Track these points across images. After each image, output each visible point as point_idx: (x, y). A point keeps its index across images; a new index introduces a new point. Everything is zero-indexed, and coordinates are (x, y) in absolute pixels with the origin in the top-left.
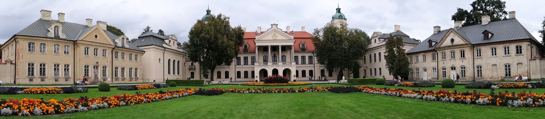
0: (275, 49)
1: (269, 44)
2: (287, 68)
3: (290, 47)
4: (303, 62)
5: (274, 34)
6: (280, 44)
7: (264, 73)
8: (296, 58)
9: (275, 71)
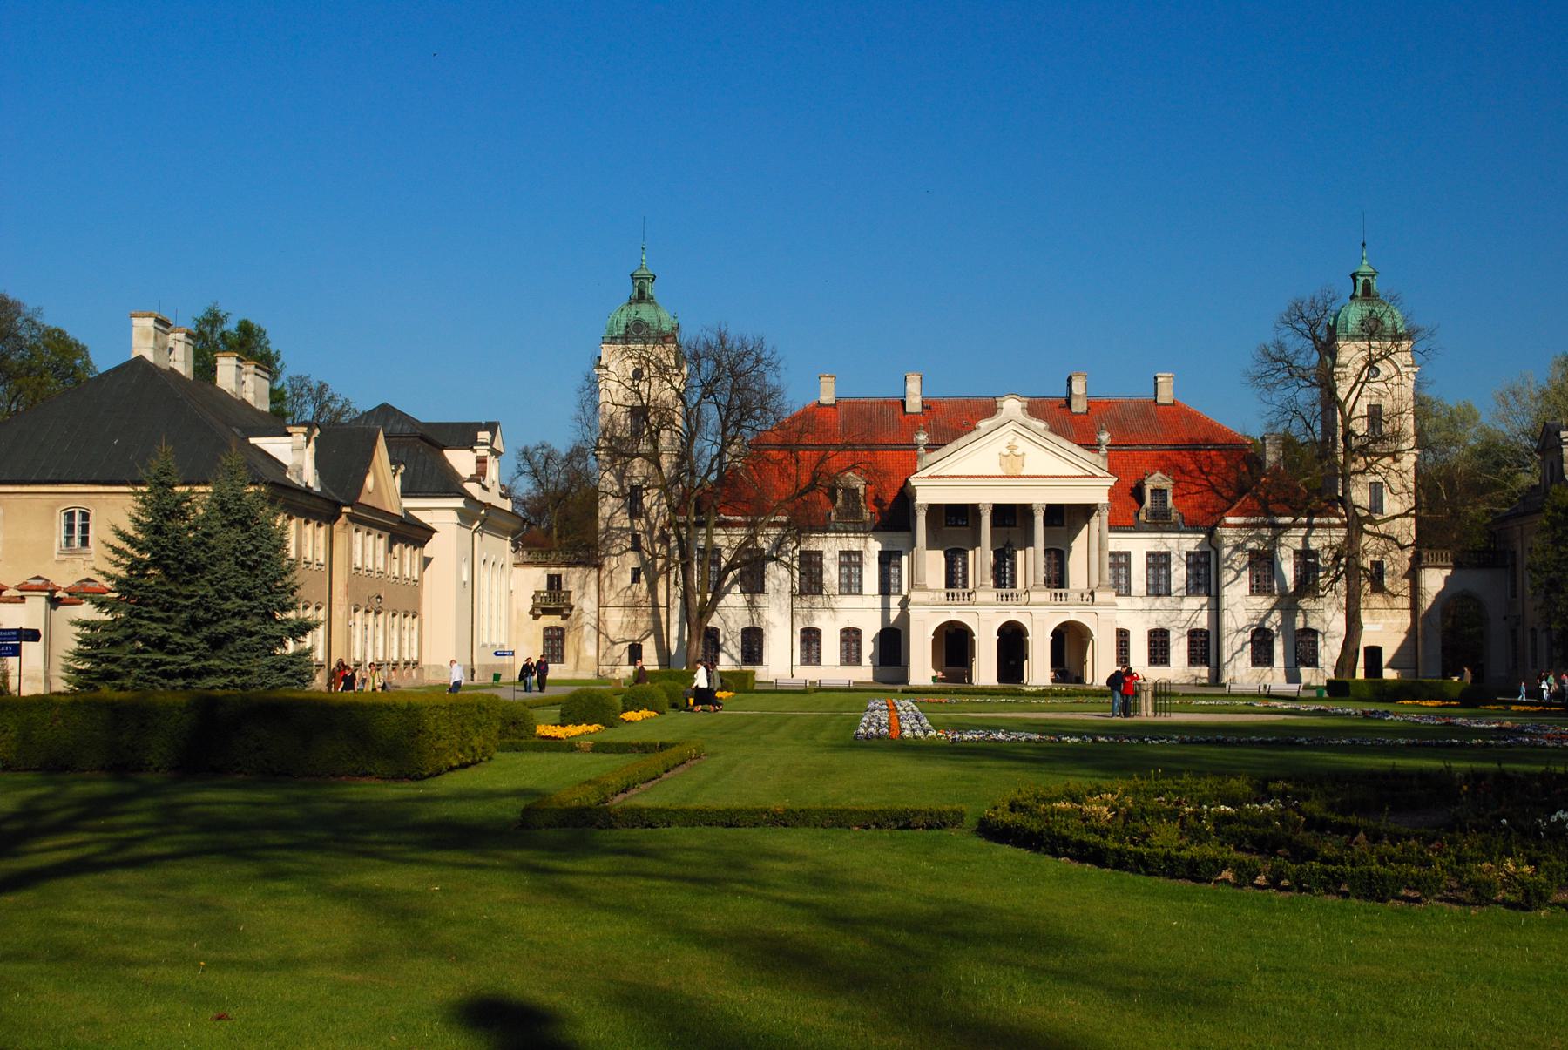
0: (1012, 518)
1: (986, 496)
2: (1073, 615)
3: (1085, 512)
4: (1160, 587)
5: (1011, 447)
6: (1039, 497)
7: (954, 644)
8: (1121, 561)
9: (1012, 641)
